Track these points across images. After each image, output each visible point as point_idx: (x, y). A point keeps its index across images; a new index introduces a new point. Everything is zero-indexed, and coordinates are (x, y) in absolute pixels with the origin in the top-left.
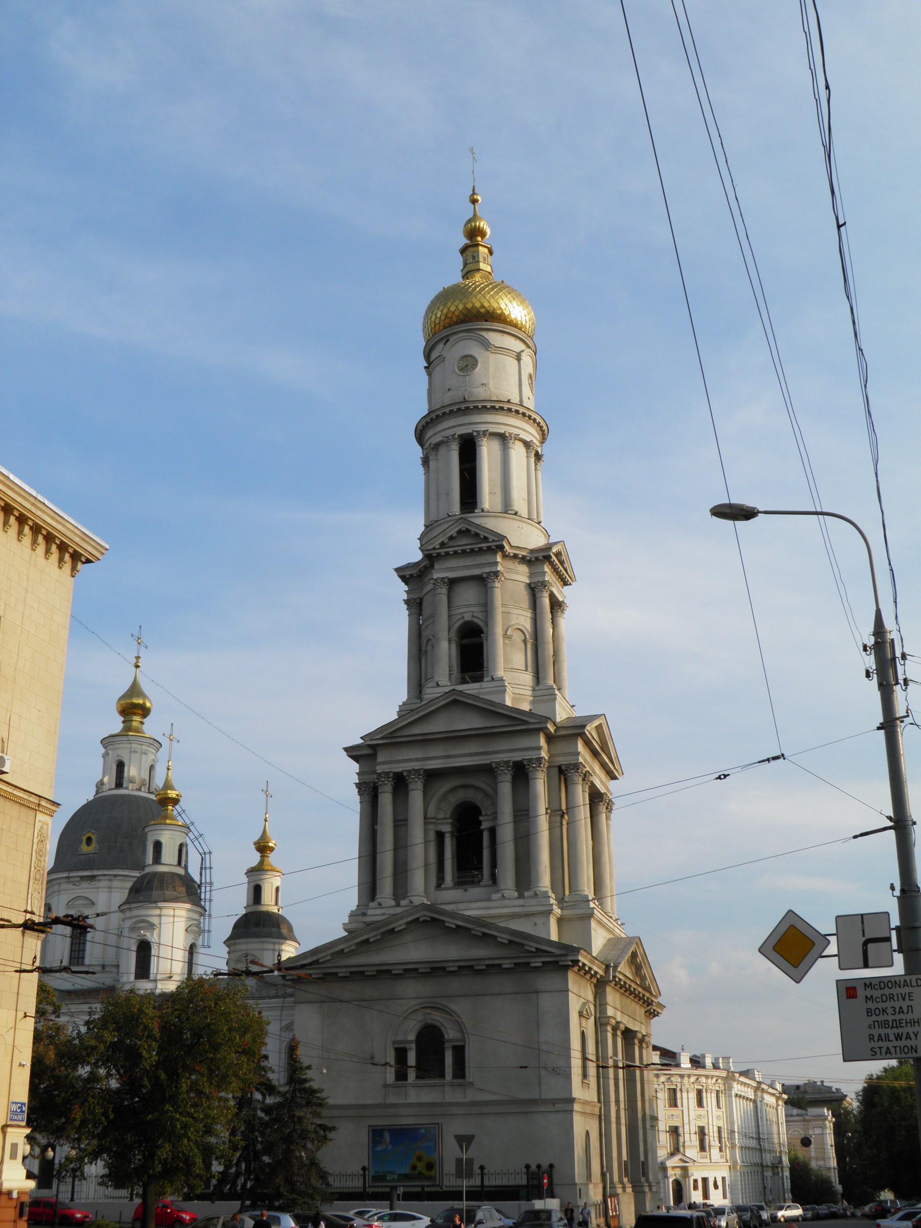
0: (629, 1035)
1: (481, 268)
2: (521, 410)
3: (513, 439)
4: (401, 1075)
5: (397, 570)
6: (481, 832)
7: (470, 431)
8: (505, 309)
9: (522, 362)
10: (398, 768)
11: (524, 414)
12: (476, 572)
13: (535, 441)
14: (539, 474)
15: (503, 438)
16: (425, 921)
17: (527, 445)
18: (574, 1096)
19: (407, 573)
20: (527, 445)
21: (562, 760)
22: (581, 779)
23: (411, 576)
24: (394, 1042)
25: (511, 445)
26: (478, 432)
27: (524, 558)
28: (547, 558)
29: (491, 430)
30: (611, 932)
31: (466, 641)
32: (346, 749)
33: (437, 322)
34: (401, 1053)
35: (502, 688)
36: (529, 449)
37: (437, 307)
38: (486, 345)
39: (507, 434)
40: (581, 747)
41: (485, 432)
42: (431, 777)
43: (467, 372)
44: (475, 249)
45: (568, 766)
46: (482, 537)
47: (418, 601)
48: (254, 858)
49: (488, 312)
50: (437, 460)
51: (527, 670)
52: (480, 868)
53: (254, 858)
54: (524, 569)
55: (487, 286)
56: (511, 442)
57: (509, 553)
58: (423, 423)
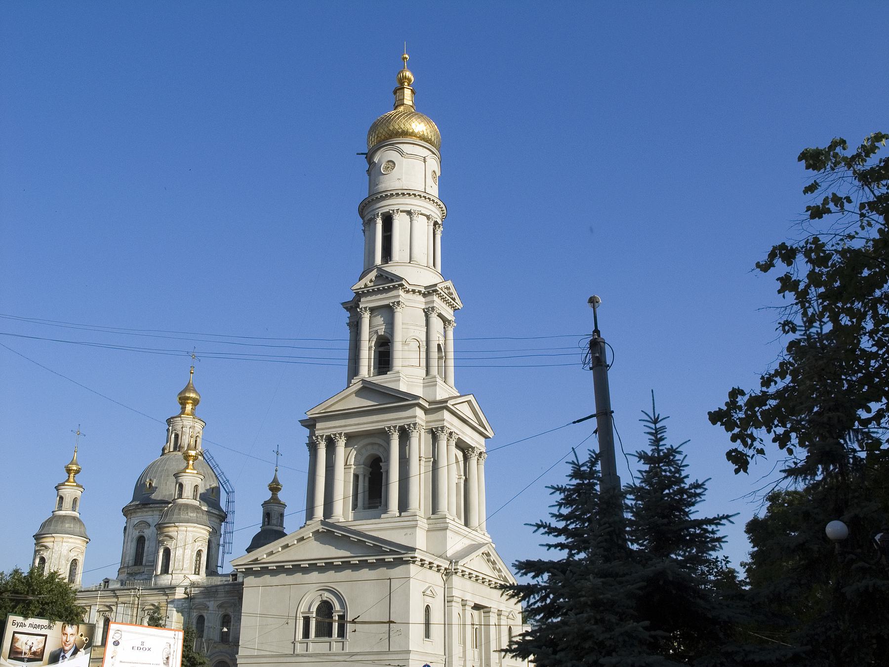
0: (477, 607)
1: (405, 103)
2: (423, 194)
4: (306, 634)
6: (381, 473)
8: (415, 129)
10: (327, 433)
11: (425, 197)
12: (386, 302)
13: (433, 214)
15: (409, 213)
16: (323, 532)
17: (428, 217)
18: (410, 649)
19: (349, 305)
21: (434, 425)
22: (446, 437)
23: (351, 307)
24: (303, 613)
27: (420, 292)
28: (436, 291)
29: (401, 209)
30: (473, 540)
31: (382, 349)
32: (299, 421)
33: (373, 140)
34: (307, 620)
35: (399, 378)
38: (401, 153)
39: (412, 211)
40: (446, 415)
42: (351, 438)
44: (401, 91)
45: (437, 428)
46: (390, 279)
47: (355, 323)
48: (268, 495)
49: (403, 131)
50: (369, 231)
51: (420, 366)
52: (381, 497)
53: (268, 495)
54: (421, 298)
55: (404, 114)
57: (409, 289)
58: (361, 207)
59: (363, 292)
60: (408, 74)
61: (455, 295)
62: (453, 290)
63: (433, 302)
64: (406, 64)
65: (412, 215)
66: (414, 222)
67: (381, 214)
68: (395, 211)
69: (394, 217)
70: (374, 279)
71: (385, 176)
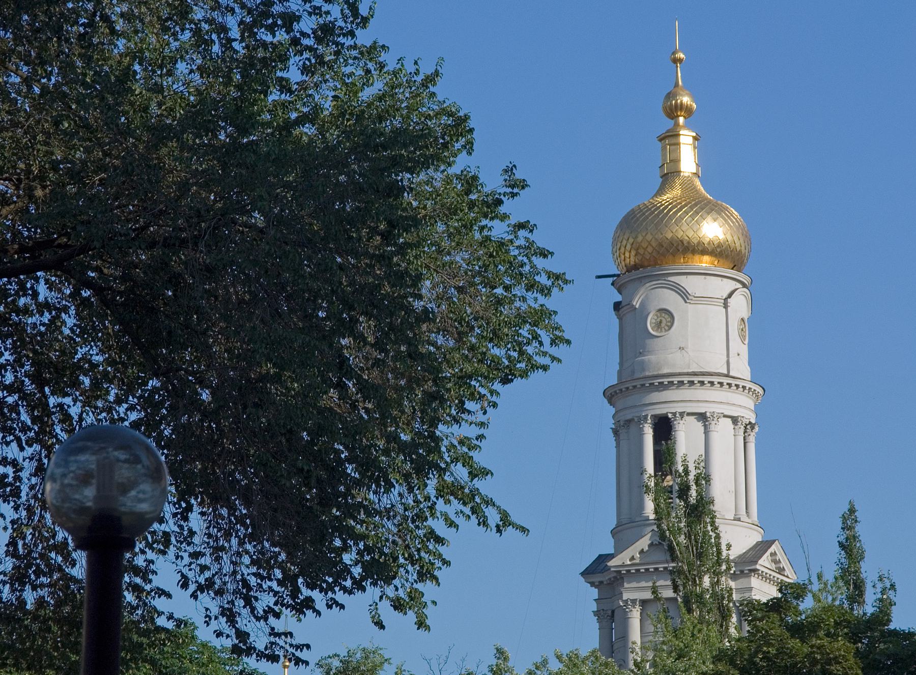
3: (715, 419)
5: (583, 574)
7: (664, 411)
9: (729, 309)
11: (730, 385)
14: (752, 447)
15: (702, 417)
17: (735, 420)
20: (735, 420)
23: (601, 582)
25: (712, 427)
26: (674, 414)
36: (736, 425)
37: (626, 237)
38: (684, 295)
39: (708, 415)
41: (682, 414)
43: (661, 331)
47: (610, 613)
56: (713, 423)
59: (628, 571)
60: (686, 100)
61: (785, 564)
62: (780, 556)
63: (750, 589)
64: (679, 75)
65: (707, 421)
66: (715, 437)
67: (652, 415)
68: (678, 415)
69: (677, 426)
70: (646, 548)
71: (656, 340)
